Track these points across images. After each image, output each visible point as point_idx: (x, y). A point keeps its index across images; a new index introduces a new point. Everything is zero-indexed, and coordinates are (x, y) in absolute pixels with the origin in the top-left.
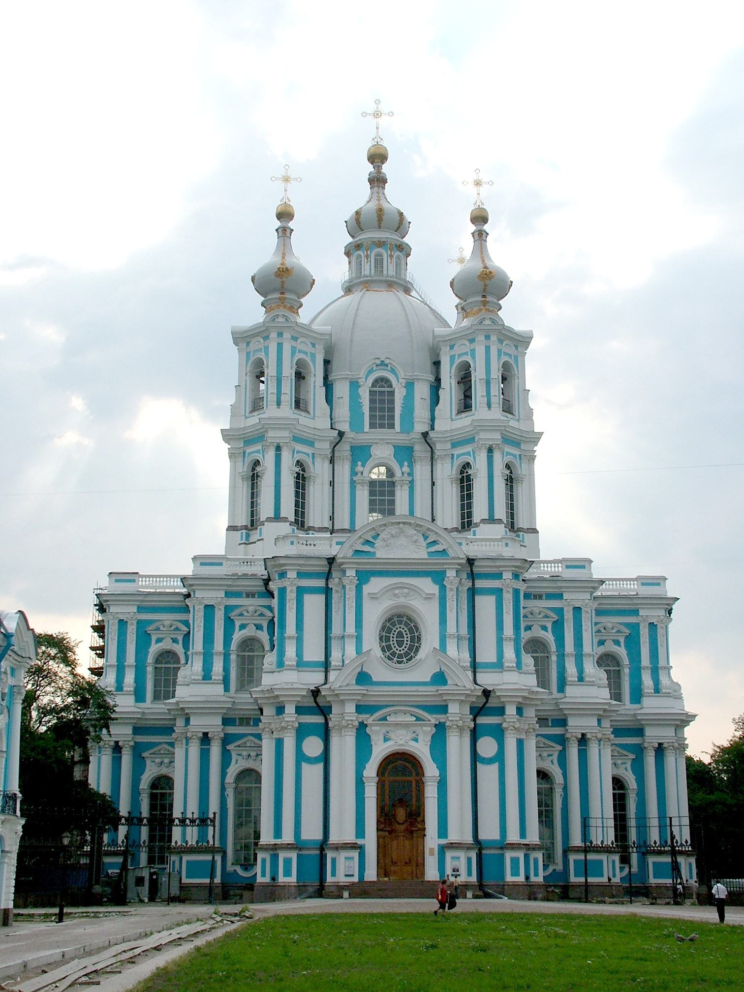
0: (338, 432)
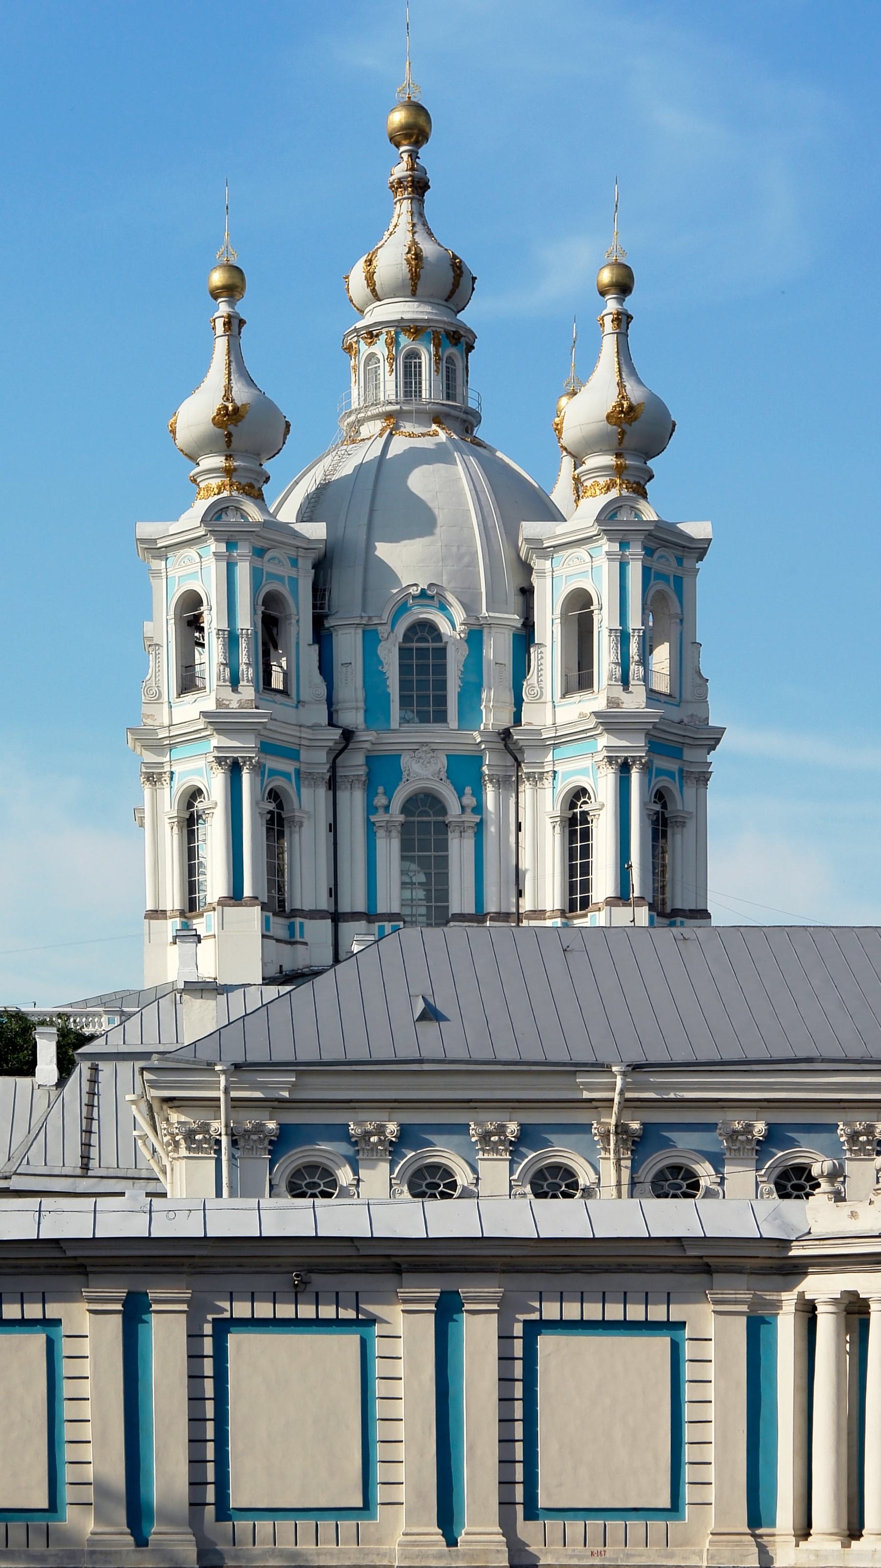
0: (340, 731)
